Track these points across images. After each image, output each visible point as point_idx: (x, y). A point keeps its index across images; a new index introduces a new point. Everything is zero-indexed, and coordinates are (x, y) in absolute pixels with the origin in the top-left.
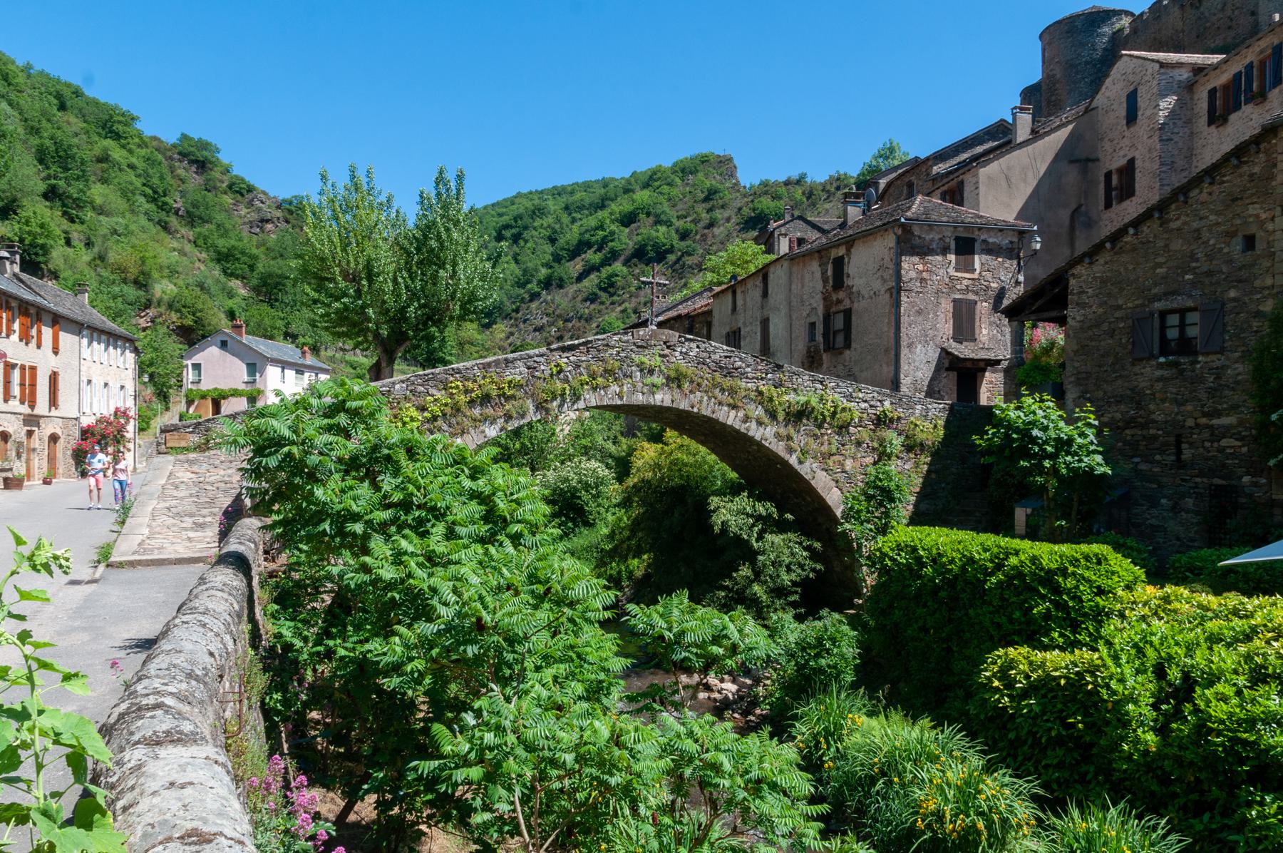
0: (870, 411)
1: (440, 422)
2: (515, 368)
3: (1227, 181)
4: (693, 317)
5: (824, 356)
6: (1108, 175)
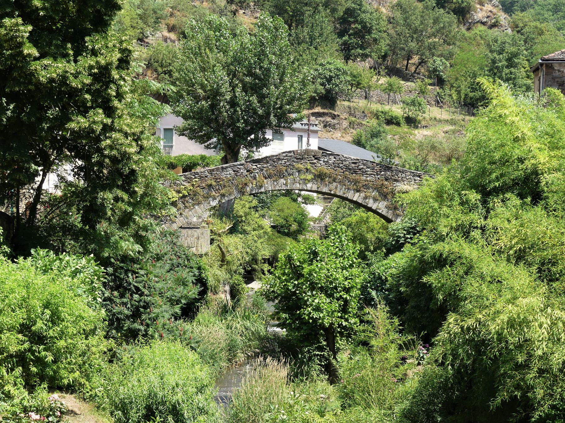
2: (227, 171)
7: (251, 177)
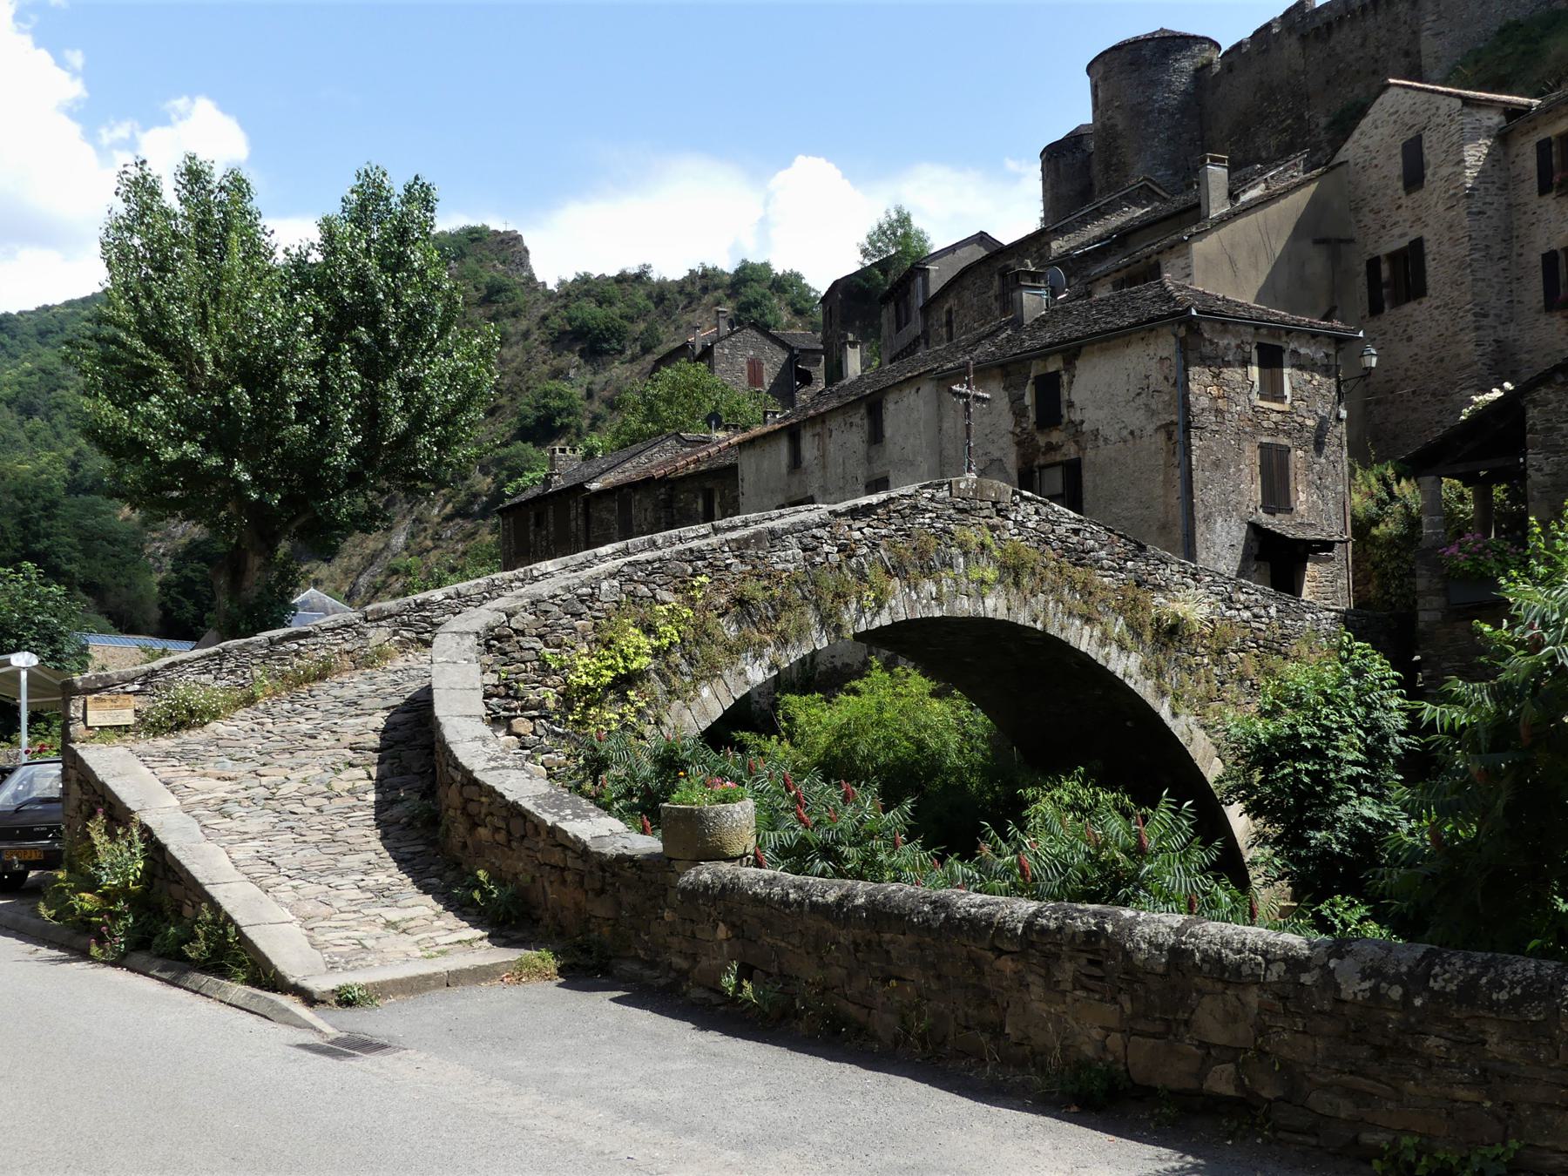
0: (1254, 625)
1: (676, 657)
2: (785, 549)
4: (671, 481)
6: (1373, 264)
7: (852, 571)
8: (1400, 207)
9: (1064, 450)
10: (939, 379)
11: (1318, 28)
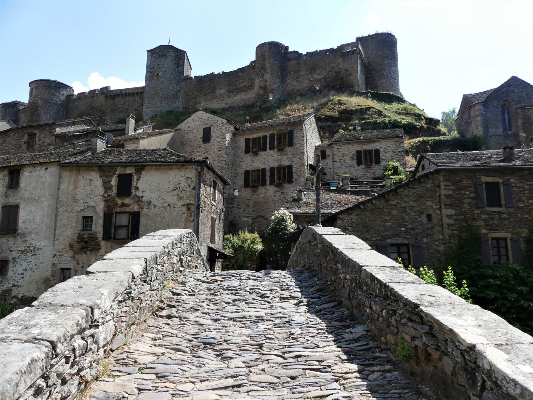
3: (417, 188)
5: (103, 243)
8: (200, 147)
9: (131, 207)
10: (61, 166)
11: (111, 96)
